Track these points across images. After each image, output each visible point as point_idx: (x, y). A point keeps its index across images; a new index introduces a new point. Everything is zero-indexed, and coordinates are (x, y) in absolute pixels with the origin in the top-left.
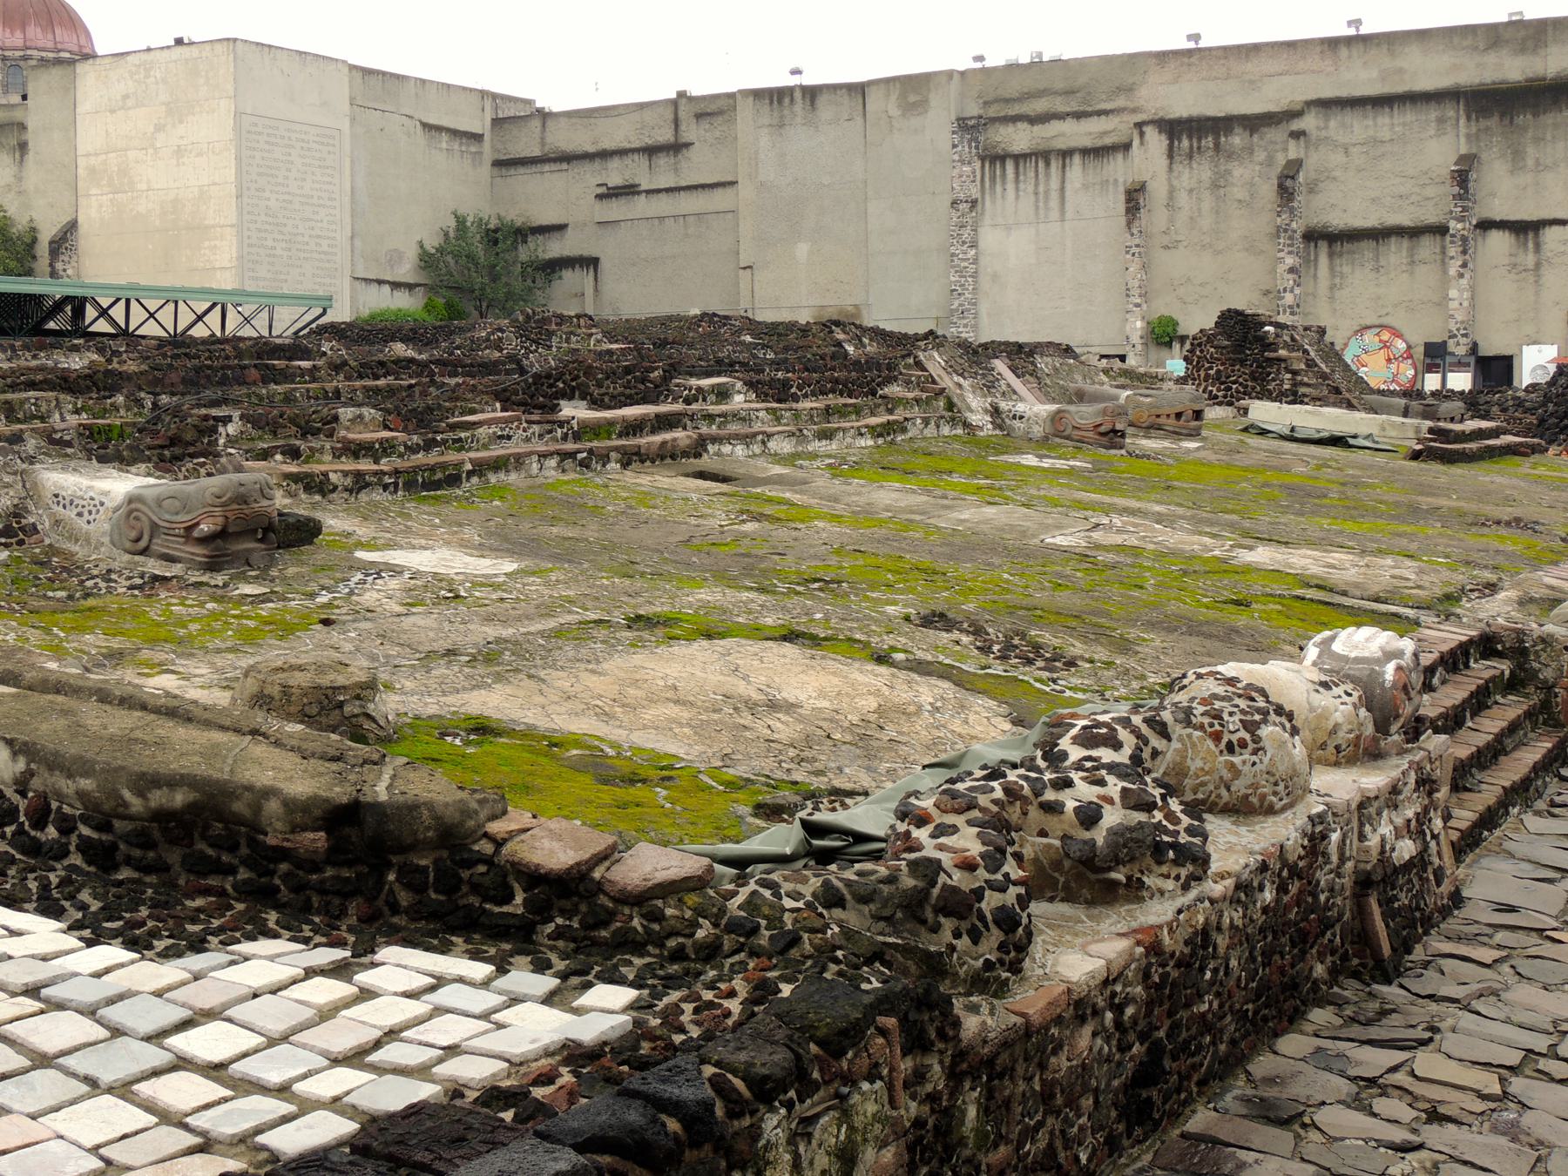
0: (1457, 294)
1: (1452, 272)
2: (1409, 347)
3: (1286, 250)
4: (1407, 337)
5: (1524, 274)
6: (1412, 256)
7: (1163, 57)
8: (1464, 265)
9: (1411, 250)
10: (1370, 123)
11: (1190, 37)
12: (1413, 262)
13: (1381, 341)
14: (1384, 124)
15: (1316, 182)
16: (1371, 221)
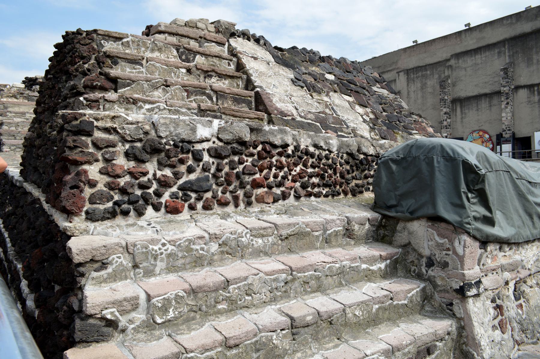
0: (506, 115)
1: (503, 106)
2: (490, 137)
3: (443, 106)
4: (490, 133)
5: (534, 104)
6: (490, 103)
7: (405, 50)
8: (508, 103)
9: (490, 102)
10: (473, 58)
11: (414, 42)
12: (491, 106)
13: (479, 135)
14: (478, 58)
15: (455, 82)
16: (475, 93)
